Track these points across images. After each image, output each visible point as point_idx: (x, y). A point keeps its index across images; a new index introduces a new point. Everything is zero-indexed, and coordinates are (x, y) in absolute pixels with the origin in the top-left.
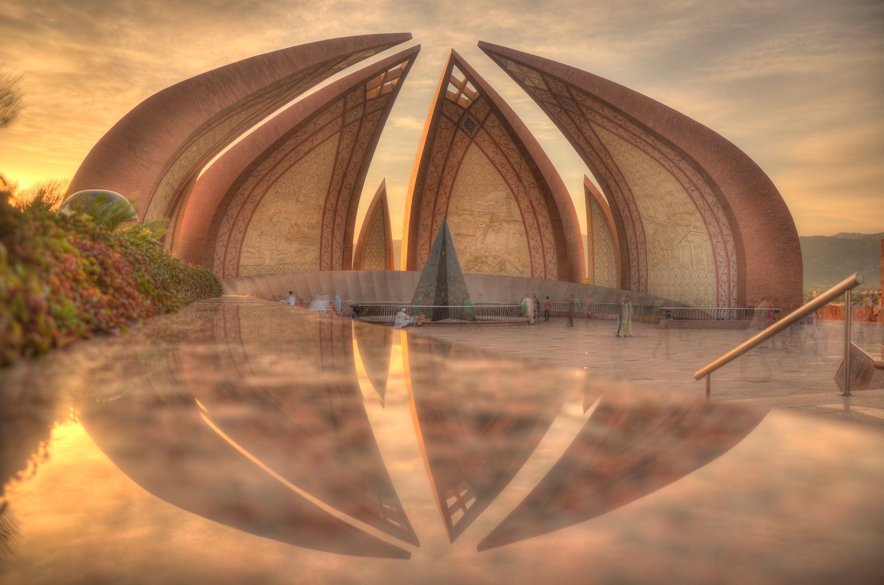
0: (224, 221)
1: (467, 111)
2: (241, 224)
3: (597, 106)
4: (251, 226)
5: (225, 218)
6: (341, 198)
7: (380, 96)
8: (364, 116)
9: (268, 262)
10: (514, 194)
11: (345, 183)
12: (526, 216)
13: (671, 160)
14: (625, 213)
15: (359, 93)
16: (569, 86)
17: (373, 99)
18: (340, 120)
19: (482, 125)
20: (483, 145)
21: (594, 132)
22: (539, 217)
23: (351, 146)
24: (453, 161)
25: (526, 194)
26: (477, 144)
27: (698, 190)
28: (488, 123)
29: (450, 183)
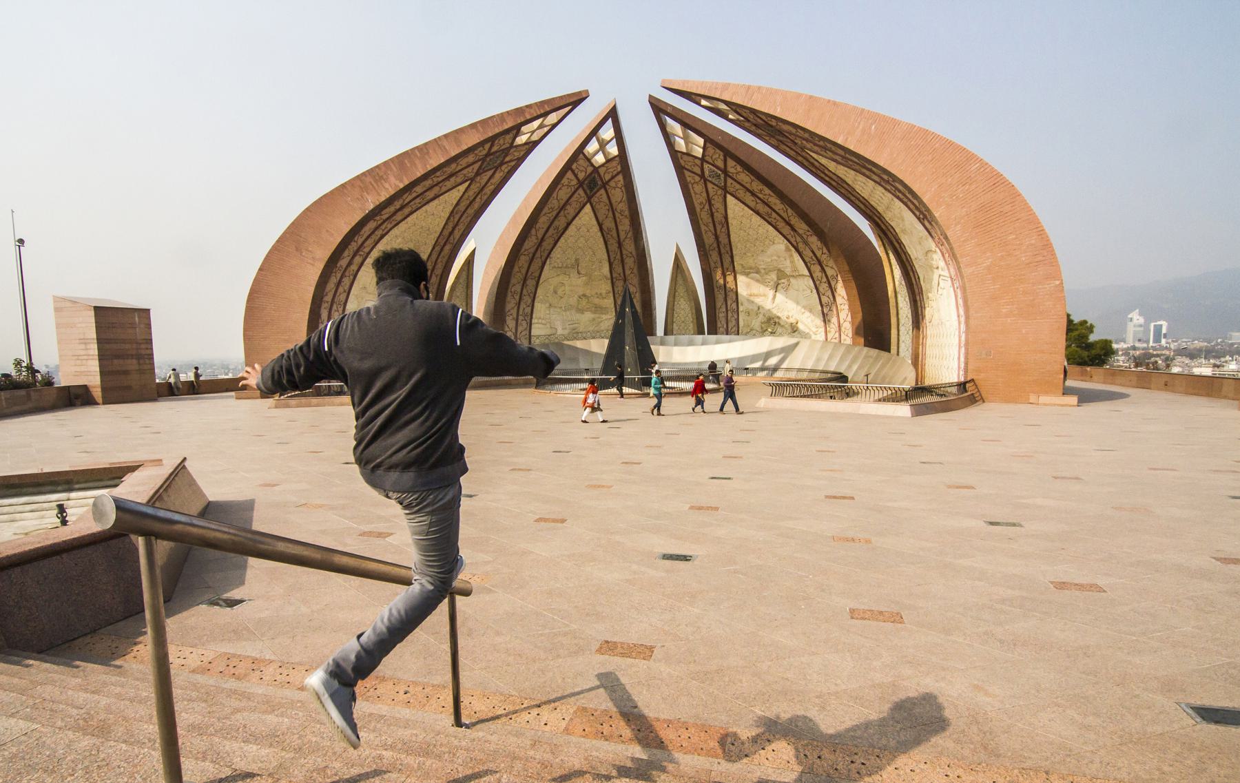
0: (509, 297)
1: (703, 159)
2: (527, 299)
3: (794, 131)
5: (509, 294)
6: (627, 268)
7: (608, 161)
9: (560, 331)
12: (812, 268)
13: (888, 182)
15: (582, 162)
16: (754, 111)
17: (603, 165)
18: (581, 191)
19: (725, 171)
22: (827, 269)
23: (611, 214)
24: (719, 216)
25: (806, 243)
29: (726, 241)
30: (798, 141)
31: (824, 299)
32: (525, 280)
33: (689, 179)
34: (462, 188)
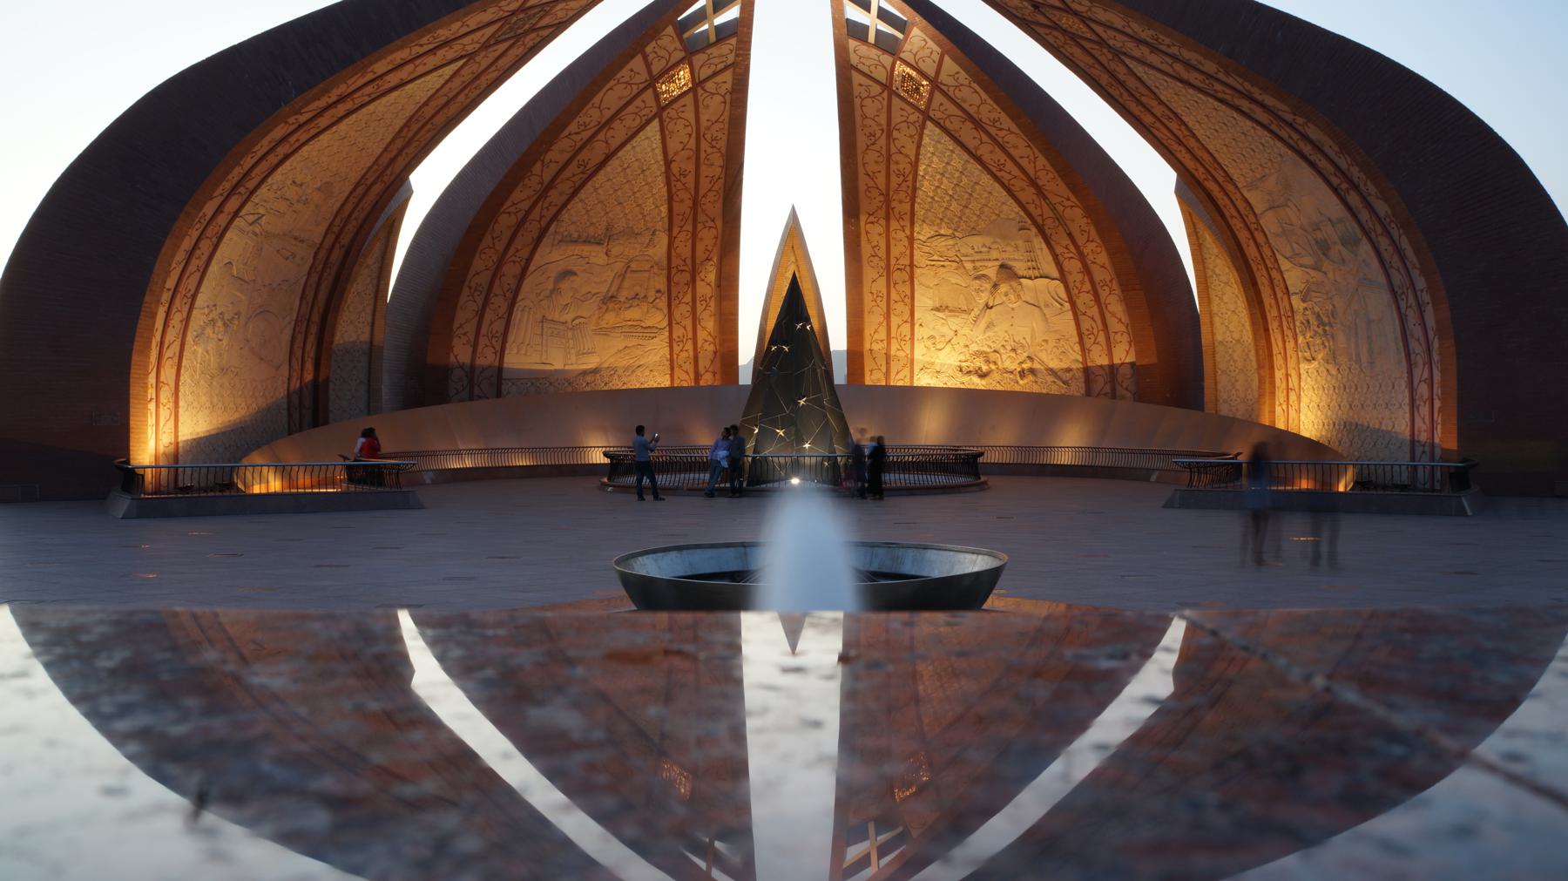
0: (464, 297)
2: (499, 303)
4: (519, 305)
5: (466, 291)
8: (697, 84)
10: (1035, 222)
11: (701, 217)
12: (1066, 265)
13: (1291, 125)
14: (1251, 252)
19: (935, 84)
20: (948, 125)
21: (1139, 79)
22: (1095, 269)
23: (692, 144)
26: (937, 124)
27: (1356, 187)
28: (943, 78)
30: (1118, 41)
31: (1086, 324)
32: (500, 264)
33: (857, 90)
34: (448, 71)
